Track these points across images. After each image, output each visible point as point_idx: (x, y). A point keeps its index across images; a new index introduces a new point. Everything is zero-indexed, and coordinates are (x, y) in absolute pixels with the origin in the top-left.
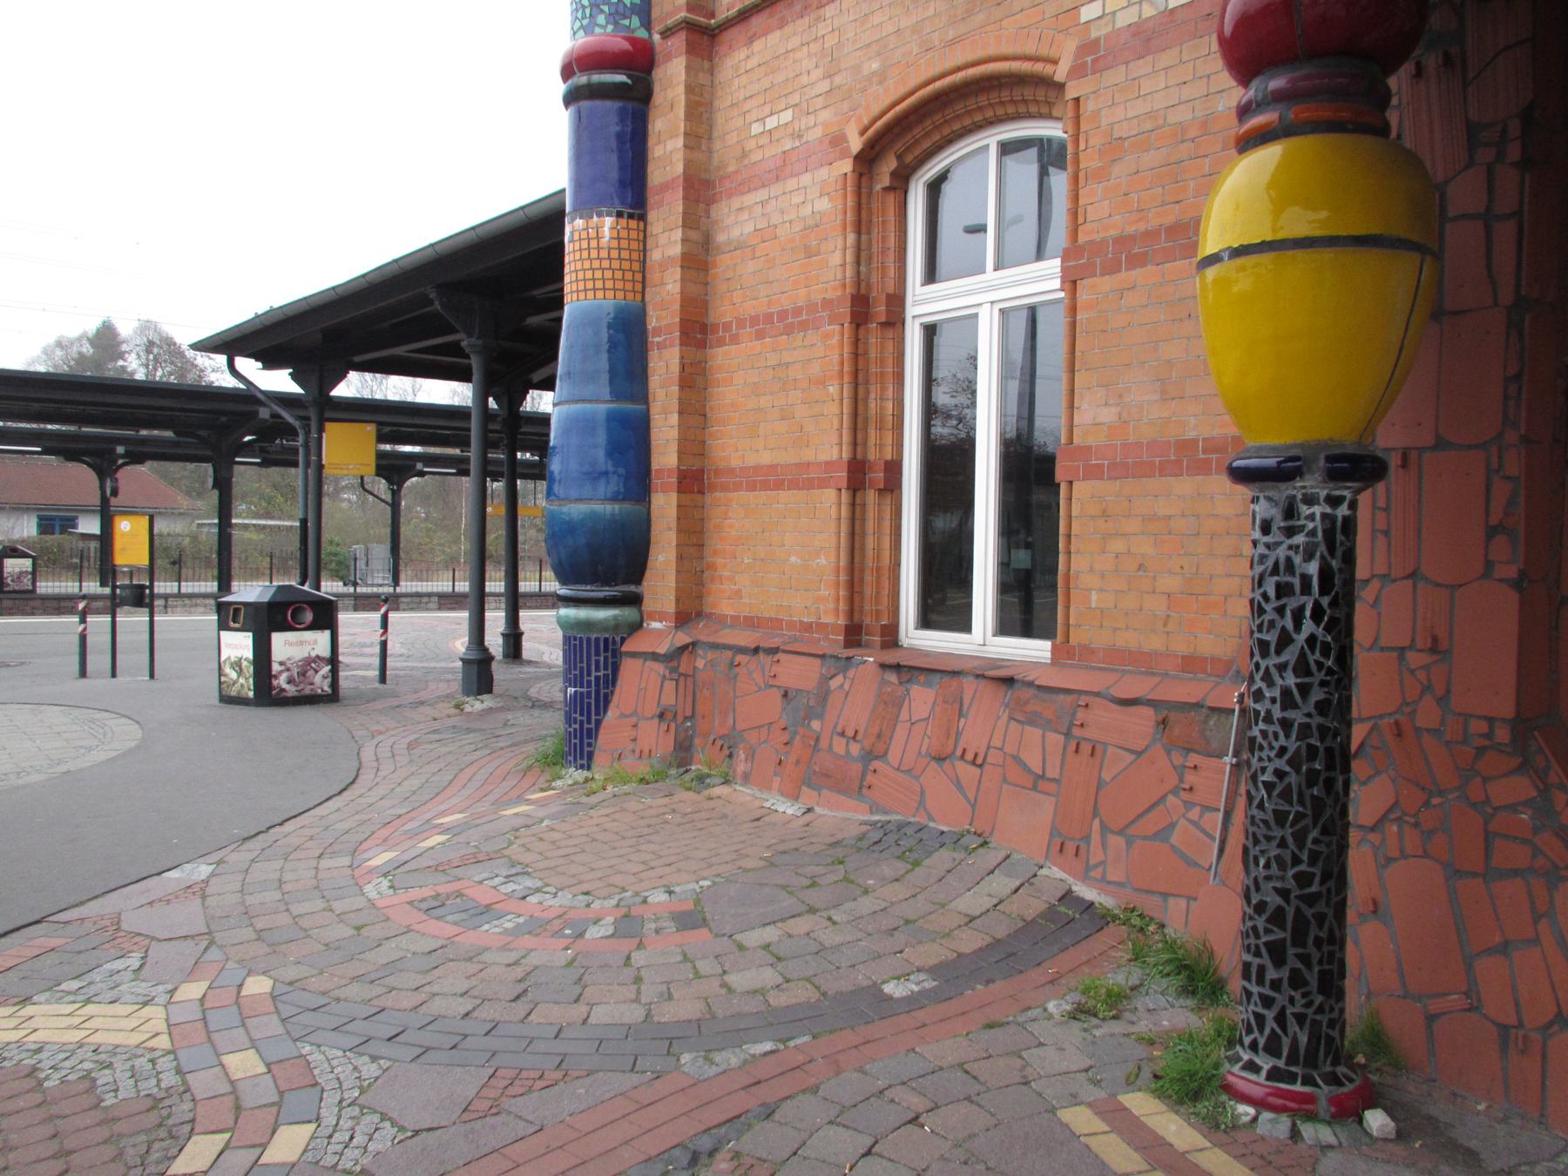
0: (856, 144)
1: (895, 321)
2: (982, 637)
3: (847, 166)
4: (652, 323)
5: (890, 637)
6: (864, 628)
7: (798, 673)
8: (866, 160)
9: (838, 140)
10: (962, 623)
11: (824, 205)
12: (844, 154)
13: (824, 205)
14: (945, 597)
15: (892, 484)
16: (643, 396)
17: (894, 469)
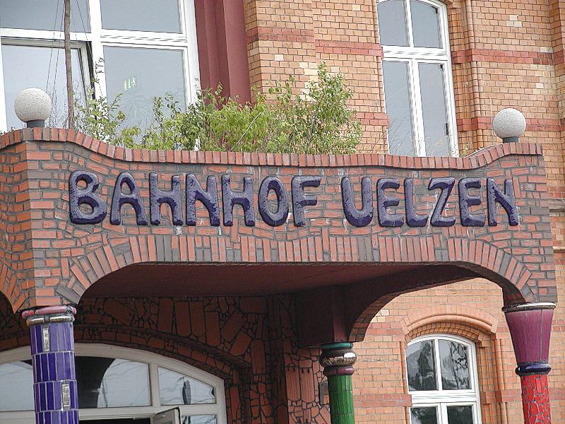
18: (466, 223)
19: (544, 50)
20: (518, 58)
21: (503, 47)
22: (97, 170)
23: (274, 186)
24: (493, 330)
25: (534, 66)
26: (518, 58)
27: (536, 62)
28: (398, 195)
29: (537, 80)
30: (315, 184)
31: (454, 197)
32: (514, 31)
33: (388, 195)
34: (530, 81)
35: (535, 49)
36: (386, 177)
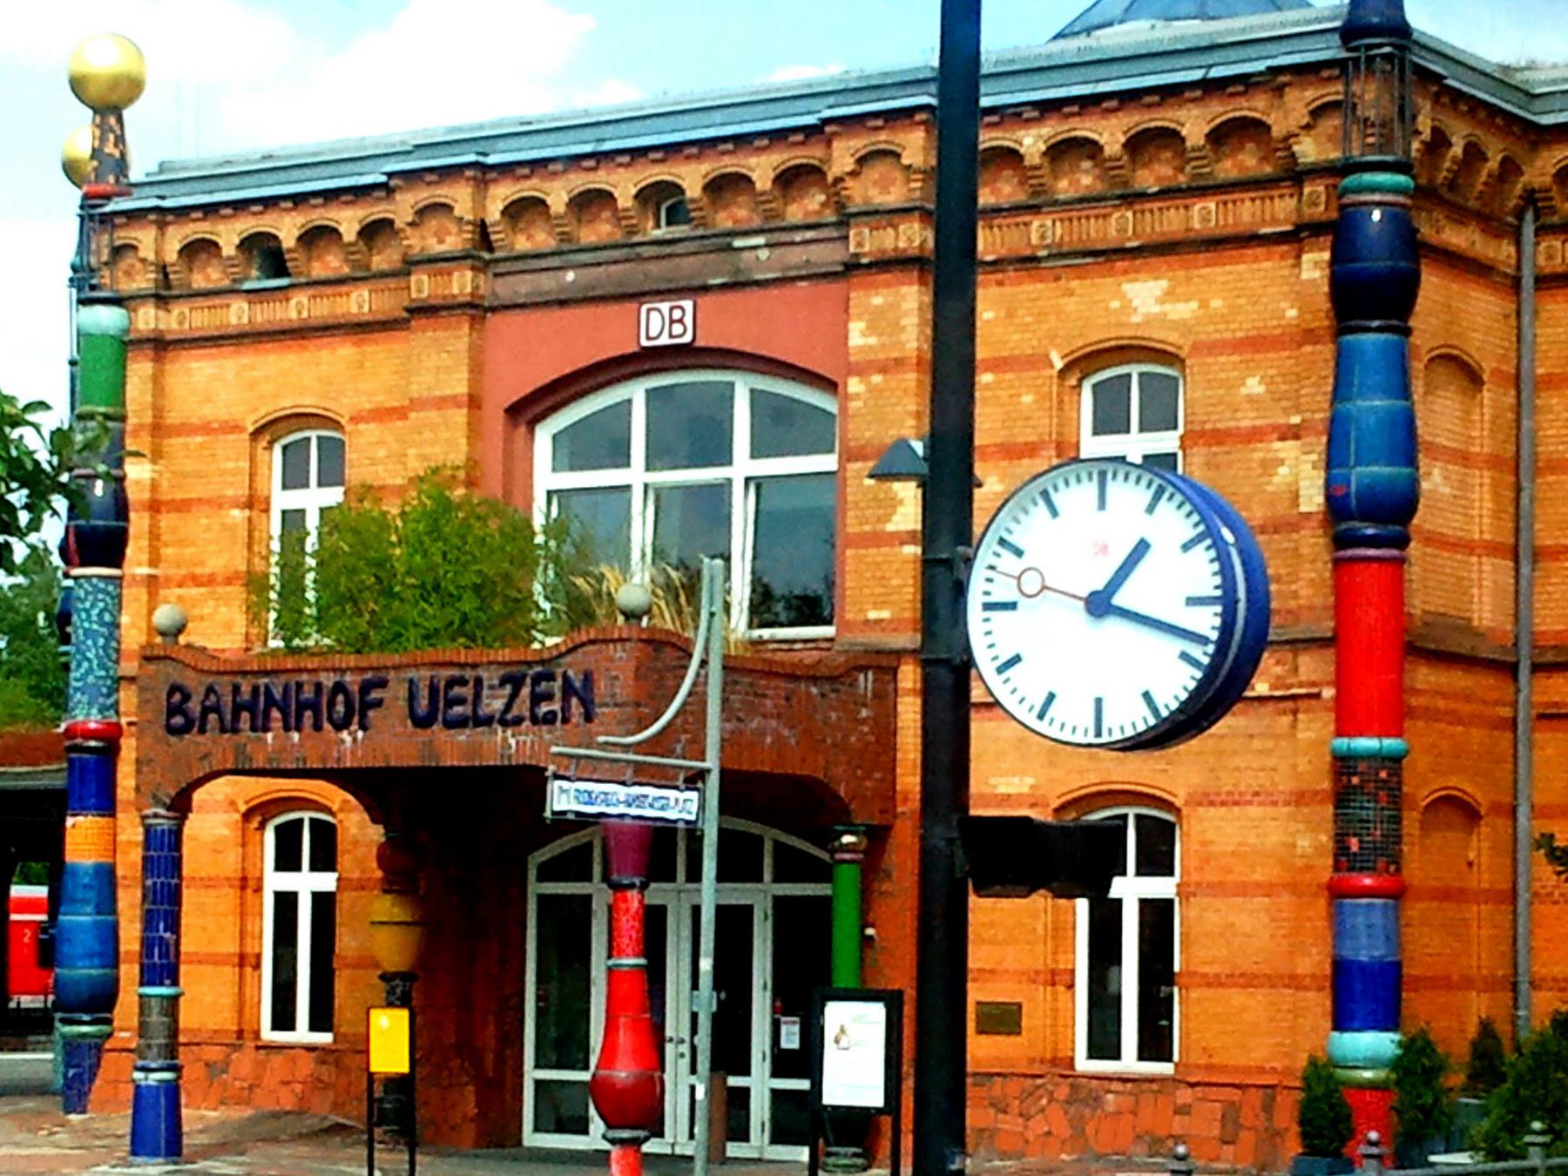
0: (243, 808)
1: (259, 890)
2: (302, 1033)
3: (237, 817)
4: (120, 872)
5: (257, 1034)
6: (244, 1034)
7: (214, 1053)
8: (247, 816)
9: (233, 803)
10: (291, 1026)
11: (226, 832)
12: (237, 811)
13: (226, 832)
14: (284, 1020)
15: (257, 966)
16: (113, 911)
17: (259, 956)
18: (535, 720)
19: (1296, 420)
20: (1254, 435)
21: (1232, 424)
22: (191, 681)
23: (339, 687)
24: (1178, 802)
25: (1278, 445)
26: (1254, 435)
27: (1282, 438)
28: (467, 691)
29: (1282, 462)
30: (383, 684)
31: (526, 691)
32: (1251, 399)
33: (457, 690)
34: (1269, 466)
35: (1282, 421)
36: (455, 672)
